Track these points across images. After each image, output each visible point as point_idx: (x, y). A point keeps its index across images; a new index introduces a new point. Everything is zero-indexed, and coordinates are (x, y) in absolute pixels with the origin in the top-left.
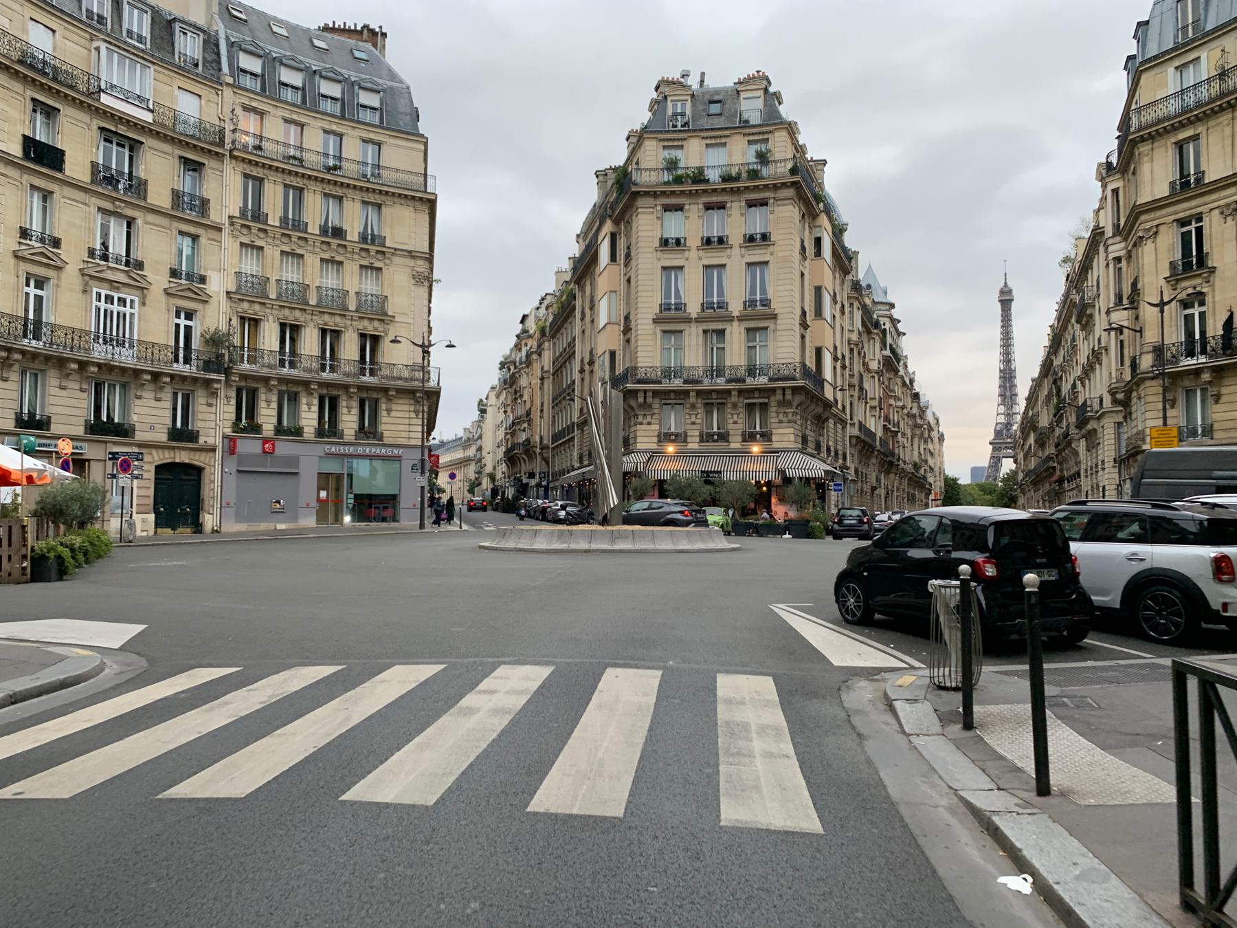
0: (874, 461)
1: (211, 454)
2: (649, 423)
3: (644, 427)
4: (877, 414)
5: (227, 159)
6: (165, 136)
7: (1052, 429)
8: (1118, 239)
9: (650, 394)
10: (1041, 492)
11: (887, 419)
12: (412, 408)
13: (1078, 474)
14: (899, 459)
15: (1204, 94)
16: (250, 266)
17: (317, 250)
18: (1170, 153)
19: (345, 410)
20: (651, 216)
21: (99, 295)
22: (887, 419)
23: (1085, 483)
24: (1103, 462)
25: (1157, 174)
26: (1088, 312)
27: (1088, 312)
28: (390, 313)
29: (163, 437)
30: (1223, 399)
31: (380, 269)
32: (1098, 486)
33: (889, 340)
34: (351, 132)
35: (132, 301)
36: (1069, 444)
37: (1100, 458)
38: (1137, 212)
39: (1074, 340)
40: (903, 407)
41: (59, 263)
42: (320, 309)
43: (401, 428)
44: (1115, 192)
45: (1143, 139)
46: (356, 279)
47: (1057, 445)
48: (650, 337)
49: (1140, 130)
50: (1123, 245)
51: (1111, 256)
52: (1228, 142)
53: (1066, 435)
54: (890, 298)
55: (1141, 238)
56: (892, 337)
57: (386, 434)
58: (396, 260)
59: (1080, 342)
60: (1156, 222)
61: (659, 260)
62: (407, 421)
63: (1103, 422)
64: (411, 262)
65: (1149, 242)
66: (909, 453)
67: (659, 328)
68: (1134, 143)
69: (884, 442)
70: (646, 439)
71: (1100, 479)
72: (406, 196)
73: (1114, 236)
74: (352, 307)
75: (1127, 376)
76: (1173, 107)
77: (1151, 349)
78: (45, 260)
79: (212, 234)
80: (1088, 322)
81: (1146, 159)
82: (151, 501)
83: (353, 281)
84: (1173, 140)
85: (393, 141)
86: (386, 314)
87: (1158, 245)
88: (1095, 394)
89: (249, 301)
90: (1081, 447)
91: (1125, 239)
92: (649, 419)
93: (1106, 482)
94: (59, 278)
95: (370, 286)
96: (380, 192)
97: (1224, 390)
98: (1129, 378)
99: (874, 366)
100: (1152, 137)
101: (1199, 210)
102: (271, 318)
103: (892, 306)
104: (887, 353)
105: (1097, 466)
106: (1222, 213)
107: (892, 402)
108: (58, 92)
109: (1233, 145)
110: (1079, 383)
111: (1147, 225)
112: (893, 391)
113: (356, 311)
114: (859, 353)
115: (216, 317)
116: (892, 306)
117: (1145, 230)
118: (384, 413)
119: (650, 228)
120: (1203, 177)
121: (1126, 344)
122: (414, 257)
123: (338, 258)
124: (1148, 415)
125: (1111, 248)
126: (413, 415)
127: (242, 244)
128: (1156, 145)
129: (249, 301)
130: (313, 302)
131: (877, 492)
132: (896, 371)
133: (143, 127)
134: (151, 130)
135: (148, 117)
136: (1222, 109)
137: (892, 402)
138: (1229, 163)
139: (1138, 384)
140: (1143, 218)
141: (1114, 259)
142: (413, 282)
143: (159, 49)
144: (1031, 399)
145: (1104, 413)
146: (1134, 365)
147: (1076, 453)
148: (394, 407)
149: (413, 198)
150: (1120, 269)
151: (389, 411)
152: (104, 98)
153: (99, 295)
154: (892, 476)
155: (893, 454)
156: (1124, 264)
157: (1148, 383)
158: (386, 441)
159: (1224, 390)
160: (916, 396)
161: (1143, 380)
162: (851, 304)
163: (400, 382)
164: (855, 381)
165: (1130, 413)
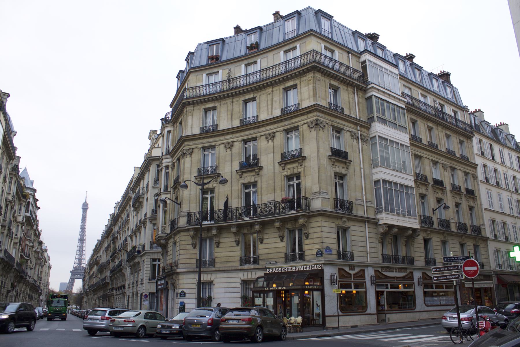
0: (12, 275)
4: (18, 247)
7: (108, 263)
8: (168, 156)
10: (98, 296)
11: (23, 251)
13: (124, 286)
14: (27, 275)
15: (219, 88)
18: (202, 113)
22: (23, 251)
23: (128, 292)
24: (142, 280)
25: (194, 123)
26: (141, 200)
27: (141, 200)
30: (221, 245)
32: (137, 293)
33: (30, 208)
36: (121, 270)
37: (140, 277)
38: (182, 140)
39: (128, 216)
40: (33, 247)
44: (169, 132)
45: (189, 104)
47: (111, 272)
49: (187, 99)
50: (170, 160)
51: (164, 165)
52: (230, 113)
53: (120, 265)
54: (35, 187)
55: (184, 153)
56: (33, 207)
59: (131, 217)
60: (192, 147)
63: (144, 258)
65: (188, 156)
66: (31, 274)
68: (185, 105)
69: (19, 265)
71: (139, 289)
73: (166, 155)
75: (168, 231)
76: (204, 91)
77: (186, 214)
80: (139, 206)
81: (190, 114)
84: (204, 107)
87: (193, 159)
88: (142, 242)
90: (127, 272)
91: (172, 157)
93: (144, 291)
97: (222, 240)
98: (169, 232)
99: (20, 219)
100: (193, 104)
101: (214, 144)
103: (35, 191)
104: (28, 214)
105: (137, 282)
106: (225, 147)
107: (27, 243)
109: (232, 114)
110: (129, 239)
111: (188, 147)
112: (28, 237)
114: (12, 208)
116: (35, 191)
117: (187, 150)
120: (217, 128)
121: (168, 212)
124: (182, 252)
125: (164, 161)
128: (195, 108)
131: (10, 294)
132: (32, 227)
136: (228, 96)
137: (27, 243)
138: (230, 122)
139: (175, 235)
140: (186, 143)
141: (166, 166)
144: (97, 250)
145: (145, 253)
146: (173, 223)
147: (124, 275)
150: (168, 173)
154: (21, 284)
155: (24, 272)
156: (170, 170)
157: (182, 234)
159: (222, 240)
160: (41, 243)
161: (179, 232)
162: (11, 178)
164: (7, 224)
165: (167, 252)
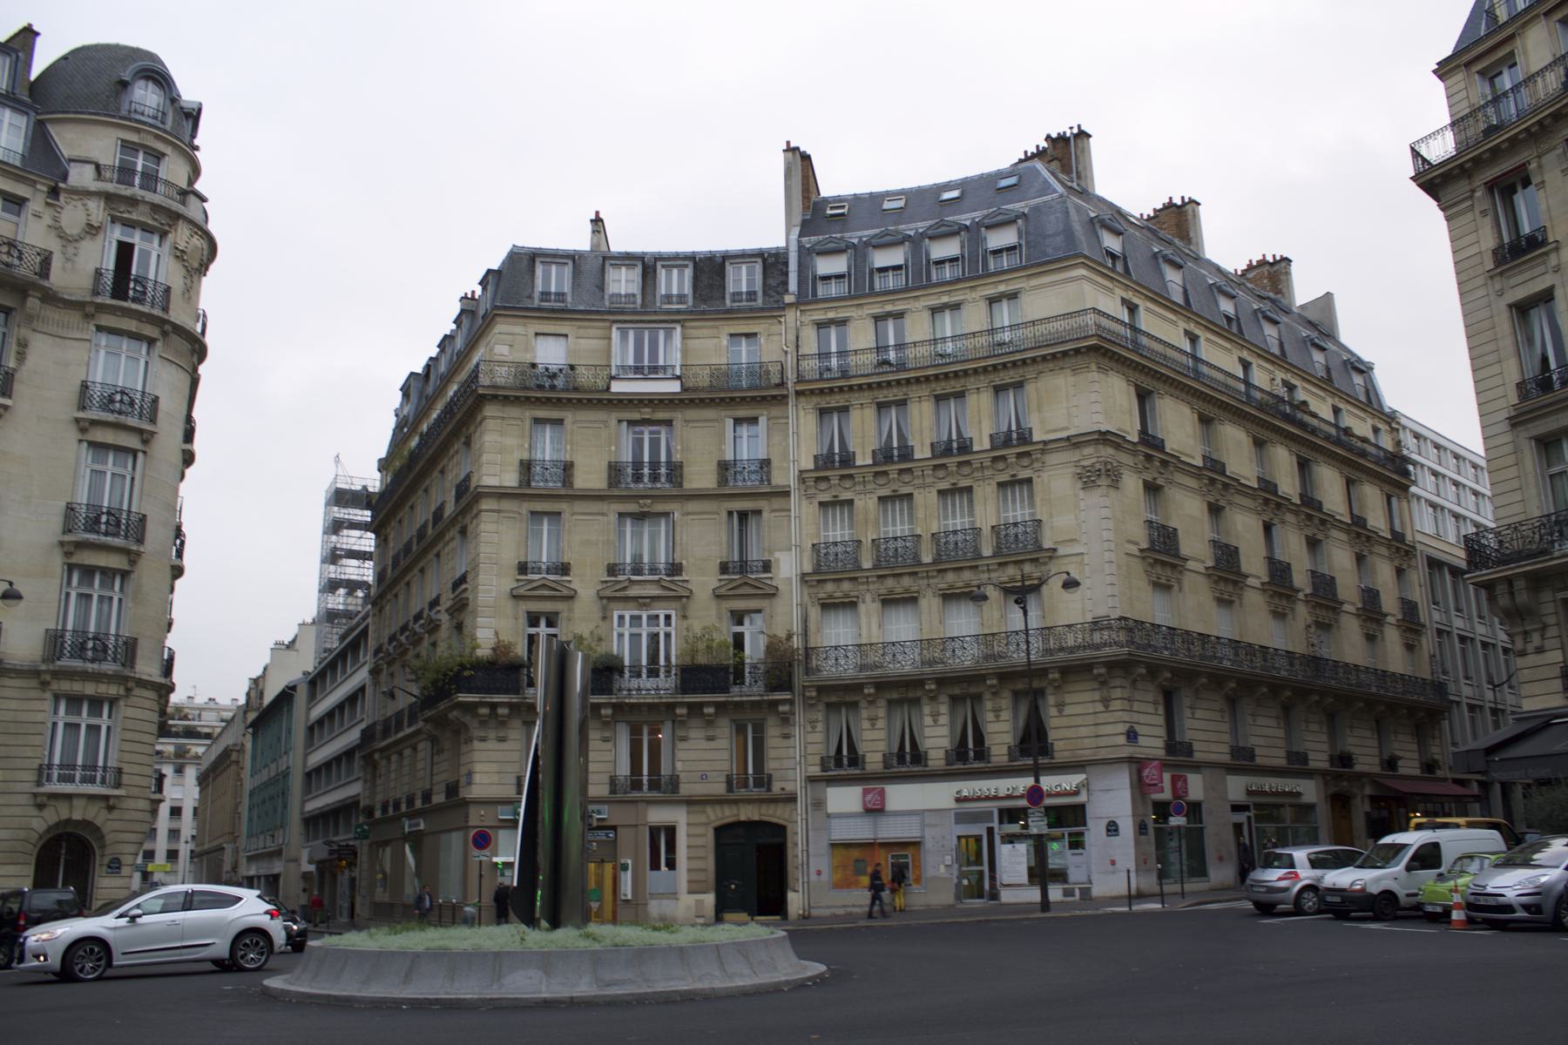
1: (789, 807)
2: (1540, 650)
3: (1532, 659)
5: (791, 401)
6: (702, 400)
9: (1520, 584)
12: (1097, 695)
16: (838, 531)
17: (929, 480)
19: (990, 716)
20: (1469, 216)
21: (621, 618)
28: (1047, 544)
29: (719, 789)
31: (1029, 481)
34: (970, 296)
35: (668, 617)
41: (565, 592)
42: (941, 565)
43: (1083, 731)
46: (991, 508)
48: (1511, 460)
57: (1058, 746)
58: (1052, 459)
61: (1500, 294)
62: (1090, 720)
64: (1074, 456)
67: (1525, 433)
70: (1537, 688)
72: (1054, 356)
74: (987, 551)
78: (546, 593)
79: (777, 503)
82: (711, 875)
83: (988, 511)
85: (1034, 282)
86: (1040, 549)
89: (834, 580)
92: (1536, 639)
94: (571, 610)
95: (1018, 512)
96: (1014, 363)
102: (868, 597)
108: (559, 400)
113: (994, 556)
115: (787, 613)
118: (1053, 711)
119: (1472, 238)
122: (1077, 446)
123: (964, 483)
126: (1100, 707)
127: (821, 504)
129: (834, 580)
130: (927, 558)
133: (671, 401)
134: (681, 401)
135: (674, 387)
142: (1080, 485)
143: (705, 301)
148: (1068, 698)
149: (1065, 354)
151: (1060, 706)
152: (616, 387)
153: (621, 618)
158: (1060, 756)
163: (1061, 655)
